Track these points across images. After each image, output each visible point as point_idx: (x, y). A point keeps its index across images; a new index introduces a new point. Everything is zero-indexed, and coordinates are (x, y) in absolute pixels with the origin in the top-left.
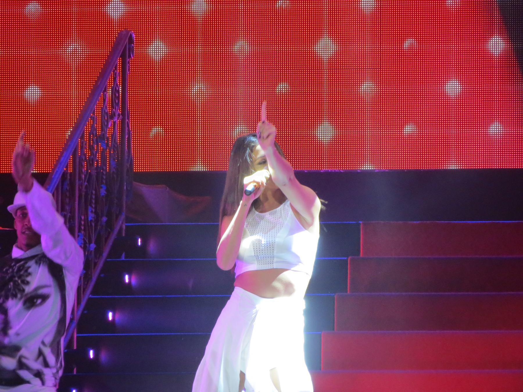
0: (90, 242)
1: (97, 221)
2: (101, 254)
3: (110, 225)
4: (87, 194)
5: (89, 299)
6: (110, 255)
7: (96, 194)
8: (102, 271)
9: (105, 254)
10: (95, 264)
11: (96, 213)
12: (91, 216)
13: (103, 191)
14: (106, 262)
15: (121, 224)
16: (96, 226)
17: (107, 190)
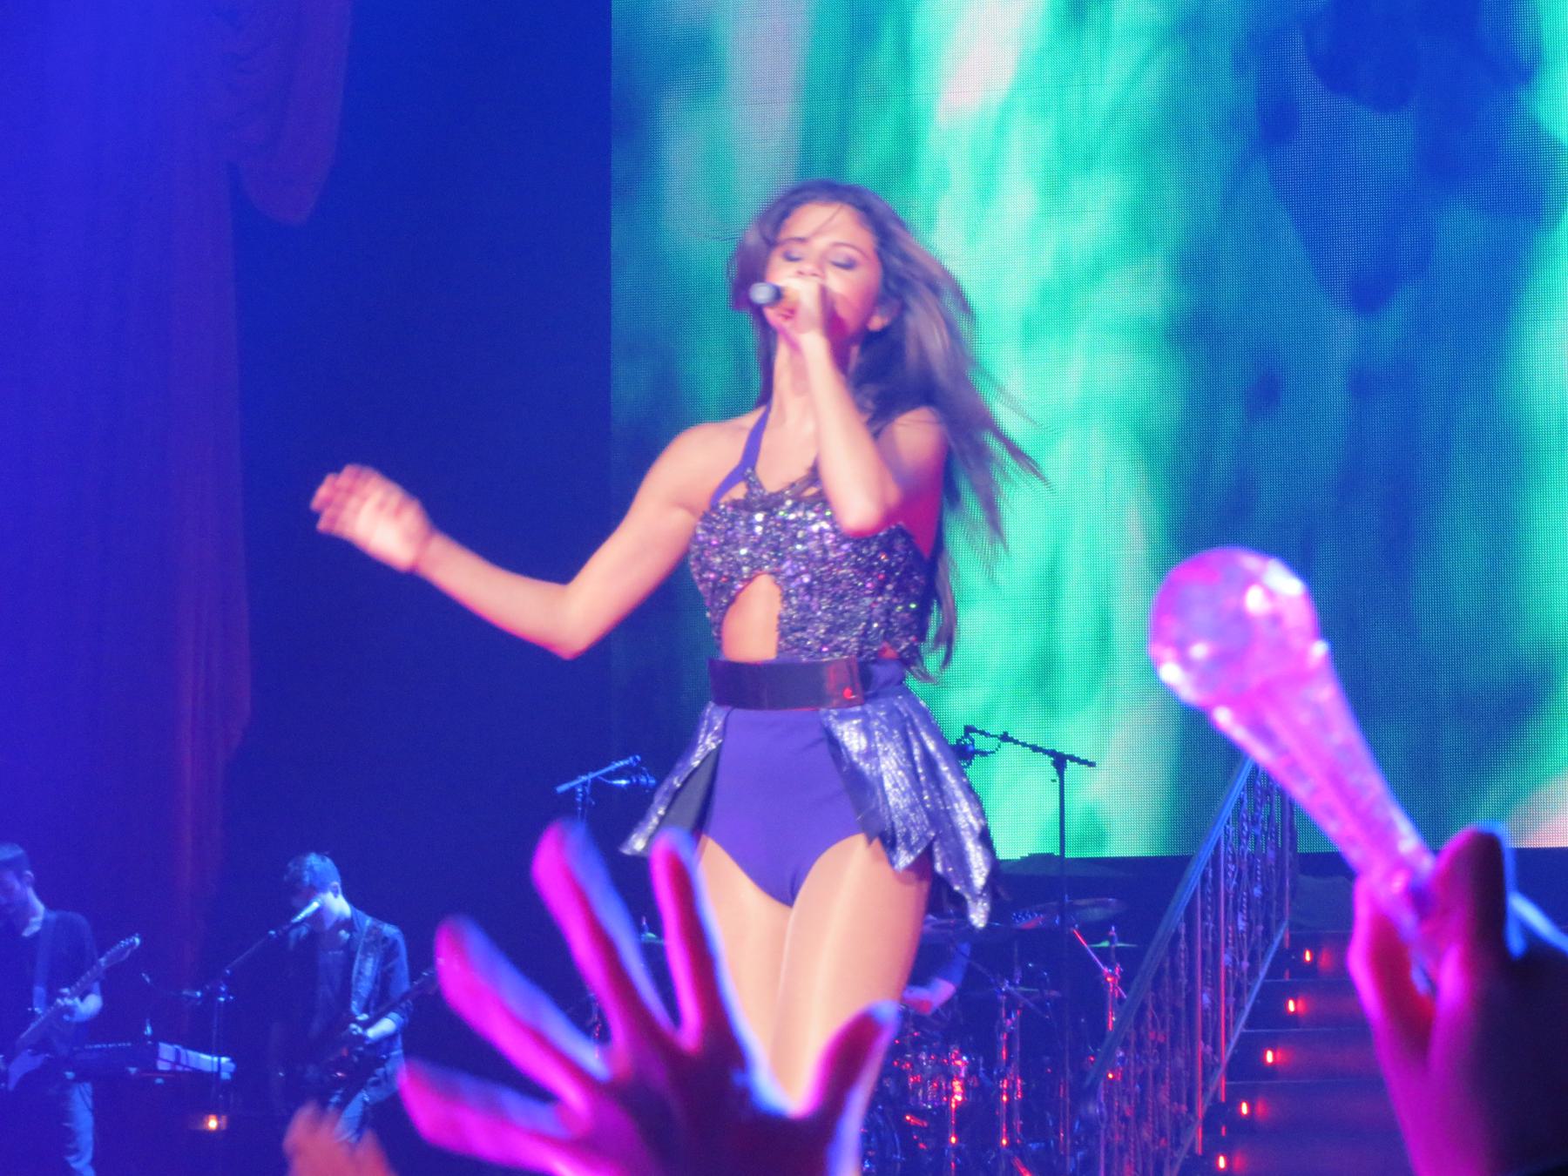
0: (1241, 959)
1: (1250, 930)
2: (1256, 974)
3: (1268, 934)
4: (1235, 899)
5: (1242, 1035)
6: (1268, 976)
7: (1248, 898)
8: (1259, 996)
9: (1262, 974)
10: (1249, 988)
11: (1248, 920)
12: (1242, 925)
13: (1257, 891)
14: (1264, 987)
15: (1281, 935)
16: (1249, 937)
17: (1263, 890)
